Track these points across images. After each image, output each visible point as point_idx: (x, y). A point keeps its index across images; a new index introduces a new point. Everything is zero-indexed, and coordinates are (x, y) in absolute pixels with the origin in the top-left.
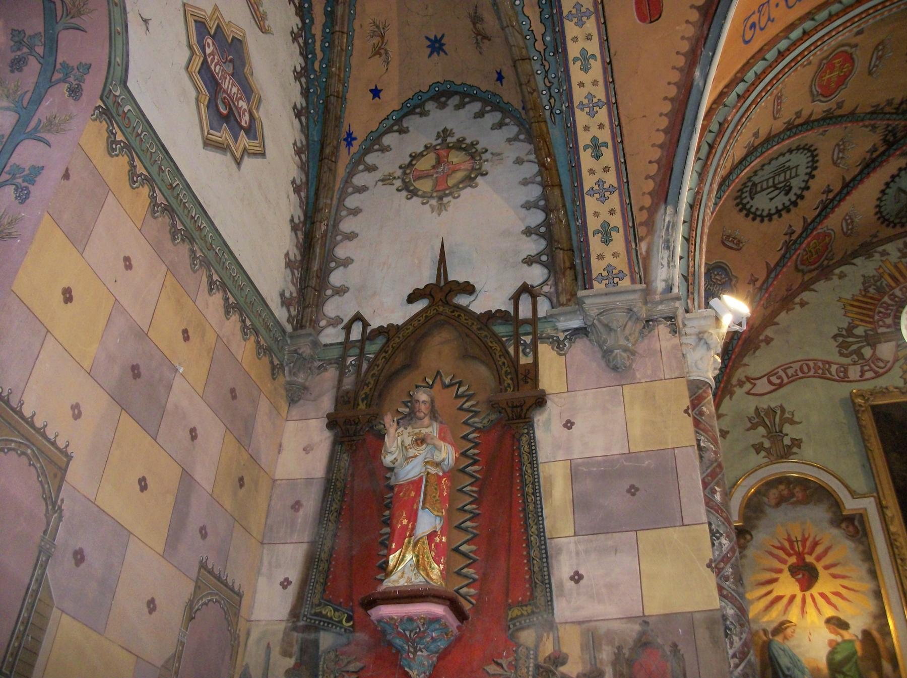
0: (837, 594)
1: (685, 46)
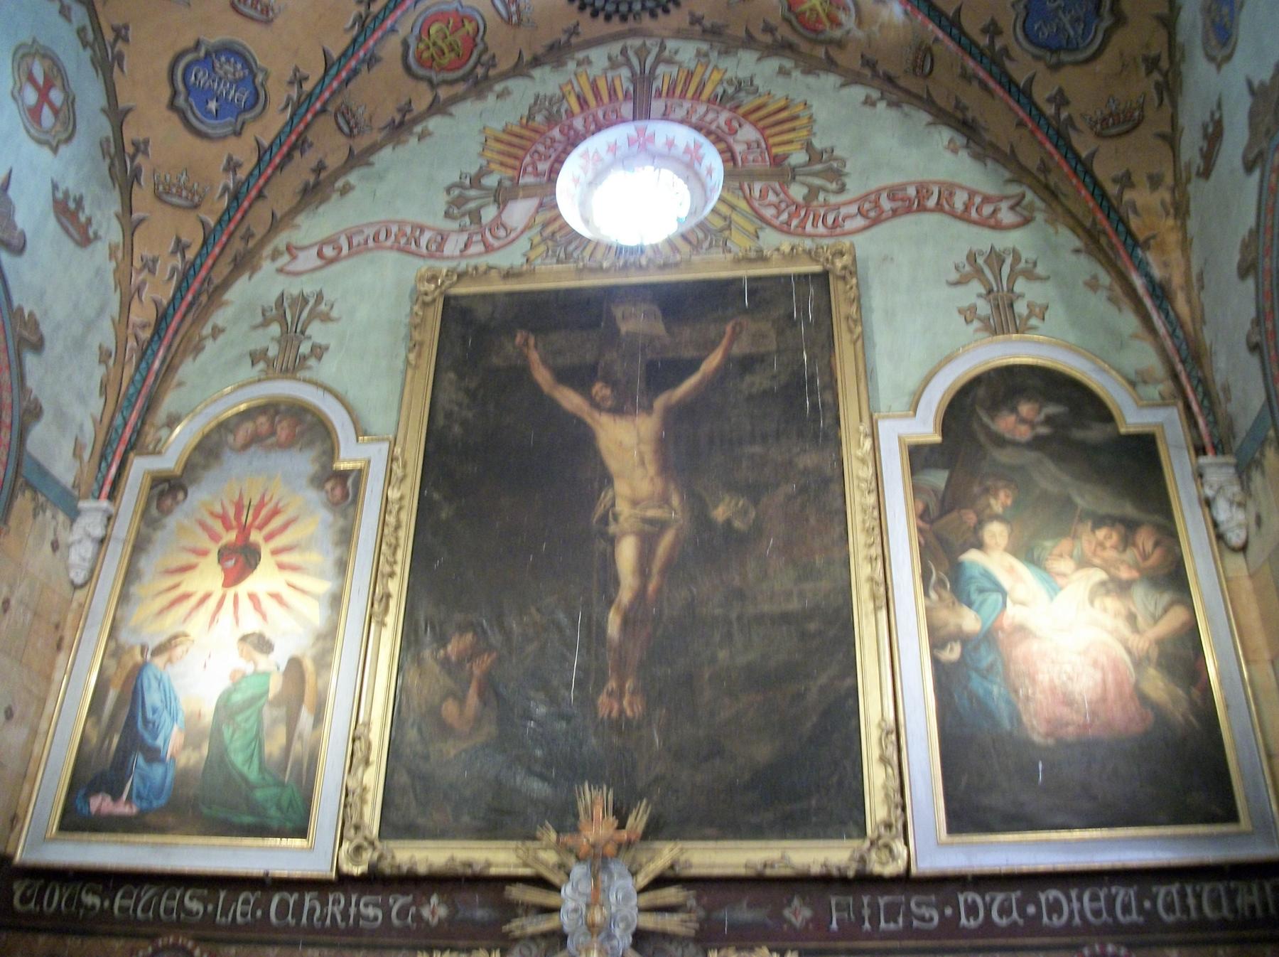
0: (276, 597)
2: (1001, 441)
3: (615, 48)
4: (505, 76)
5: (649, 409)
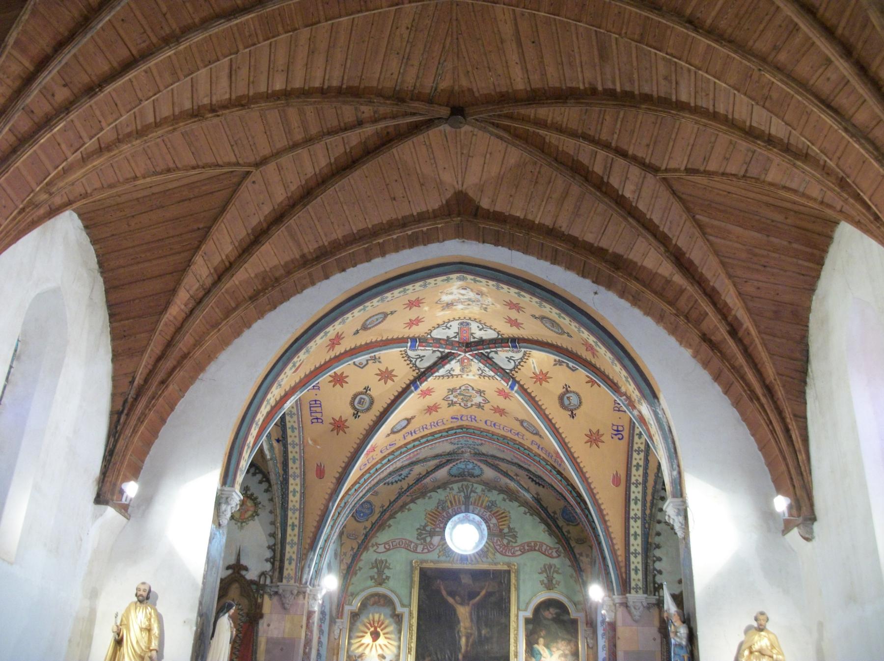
1: (329, 491)
2: (546, 619)
3: (460, 484)
4: (430, 491)
5: (468, 604)
